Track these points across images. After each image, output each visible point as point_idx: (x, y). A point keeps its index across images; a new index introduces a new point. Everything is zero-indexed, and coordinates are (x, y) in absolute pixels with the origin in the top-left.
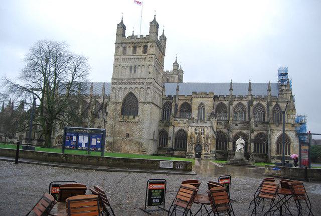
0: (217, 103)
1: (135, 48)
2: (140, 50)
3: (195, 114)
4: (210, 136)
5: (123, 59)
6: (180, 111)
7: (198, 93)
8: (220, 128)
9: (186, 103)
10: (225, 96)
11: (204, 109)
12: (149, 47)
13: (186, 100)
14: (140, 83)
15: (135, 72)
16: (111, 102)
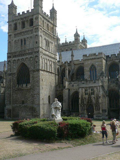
0: (109, 63)
1: (23, 24)
2: (27, 25)
3: (87, 75)
4: (100, 96)
5: (15, 35)
6: (77, 75)
7: (88, 55)
8: (111, 86)
9: (81, 66)
10: (117, 55)
11: (96, 69)
12: (34, 20)
13: (81, 64)
14: (29, 54)
15: (25, 44)
16: (8, 74)
